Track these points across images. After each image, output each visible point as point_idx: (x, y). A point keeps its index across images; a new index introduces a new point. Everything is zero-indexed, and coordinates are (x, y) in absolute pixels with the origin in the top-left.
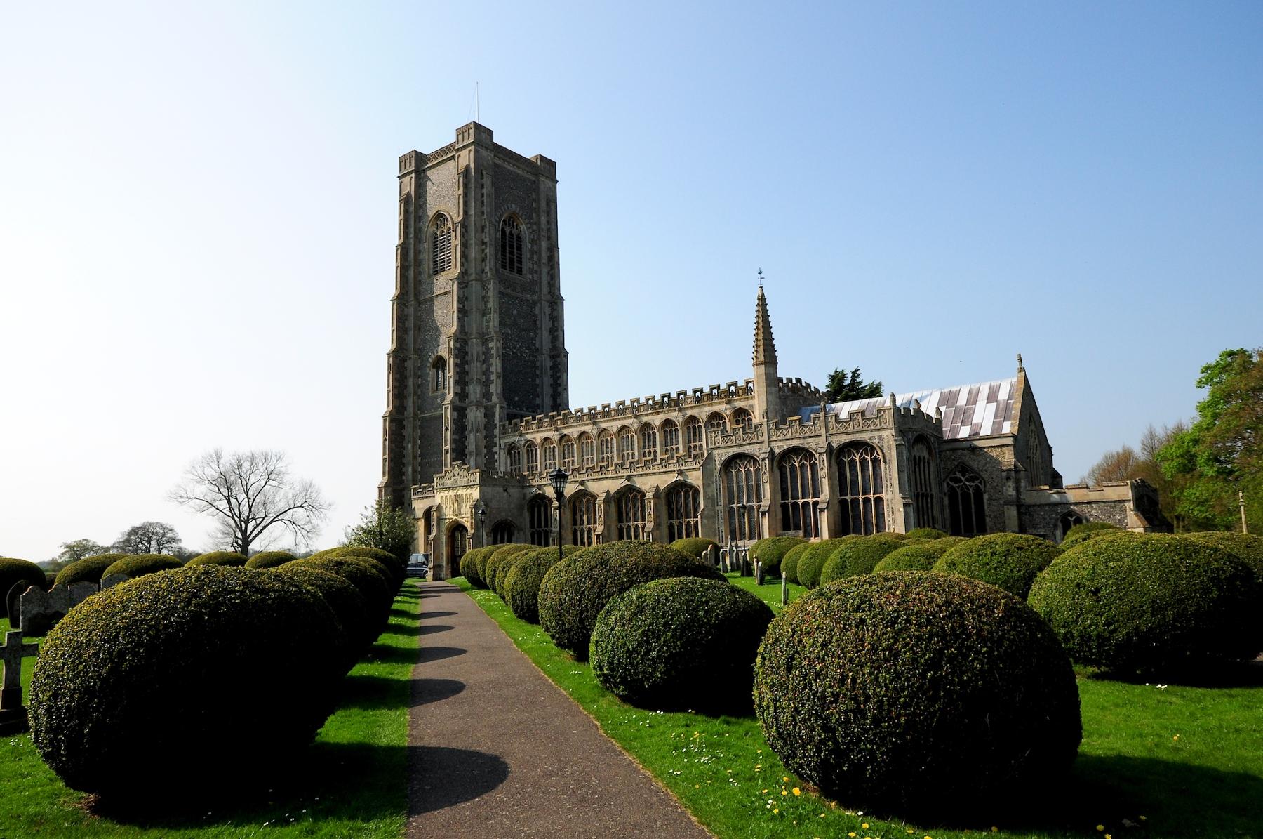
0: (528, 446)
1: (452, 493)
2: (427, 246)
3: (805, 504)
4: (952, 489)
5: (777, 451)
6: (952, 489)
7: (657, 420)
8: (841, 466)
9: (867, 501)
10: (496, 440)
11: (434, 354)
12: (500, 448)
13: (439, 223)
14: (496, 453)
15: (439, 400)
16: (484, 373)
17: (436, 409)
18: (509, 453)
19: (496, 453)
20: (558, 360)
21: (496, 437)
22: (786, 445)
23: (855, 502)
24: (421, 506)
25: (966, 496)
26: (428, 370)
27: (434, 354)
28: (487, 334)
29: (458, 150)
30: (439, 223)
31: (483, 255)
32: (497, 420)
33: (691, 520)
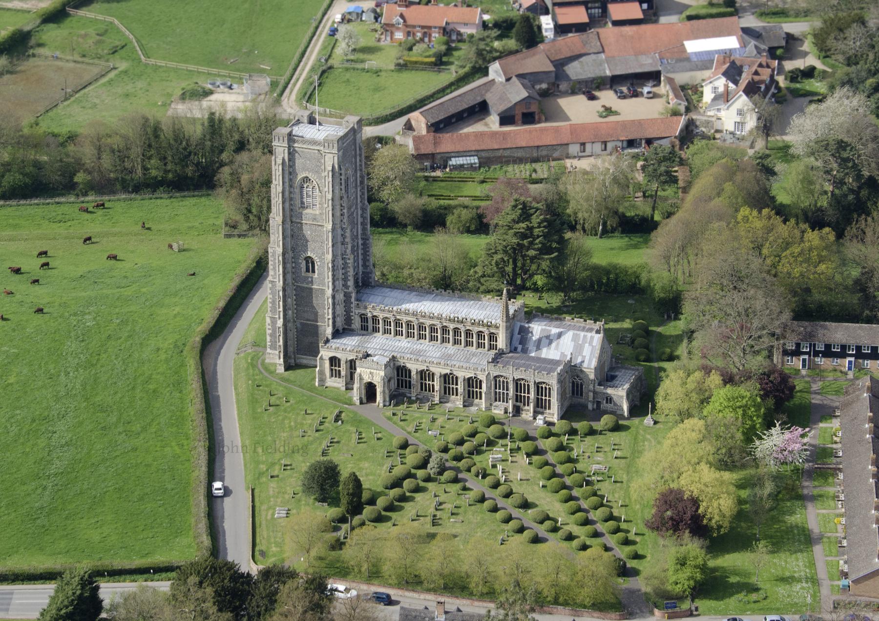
1: (369, 371)
3: (524, 396)
4: (573, 382)
5: (516, 378)
6: (573, 382)
7: (452, 326)
8: (538, 387)
9: (545, 400)
10: (353, 310)
16: (343, 274)
18: (361, 318)
20: (368, 242)
22: (519, 377)
23: (542, 399)
25: (577, 384)
32: (353, 300)
33: (478, 390)
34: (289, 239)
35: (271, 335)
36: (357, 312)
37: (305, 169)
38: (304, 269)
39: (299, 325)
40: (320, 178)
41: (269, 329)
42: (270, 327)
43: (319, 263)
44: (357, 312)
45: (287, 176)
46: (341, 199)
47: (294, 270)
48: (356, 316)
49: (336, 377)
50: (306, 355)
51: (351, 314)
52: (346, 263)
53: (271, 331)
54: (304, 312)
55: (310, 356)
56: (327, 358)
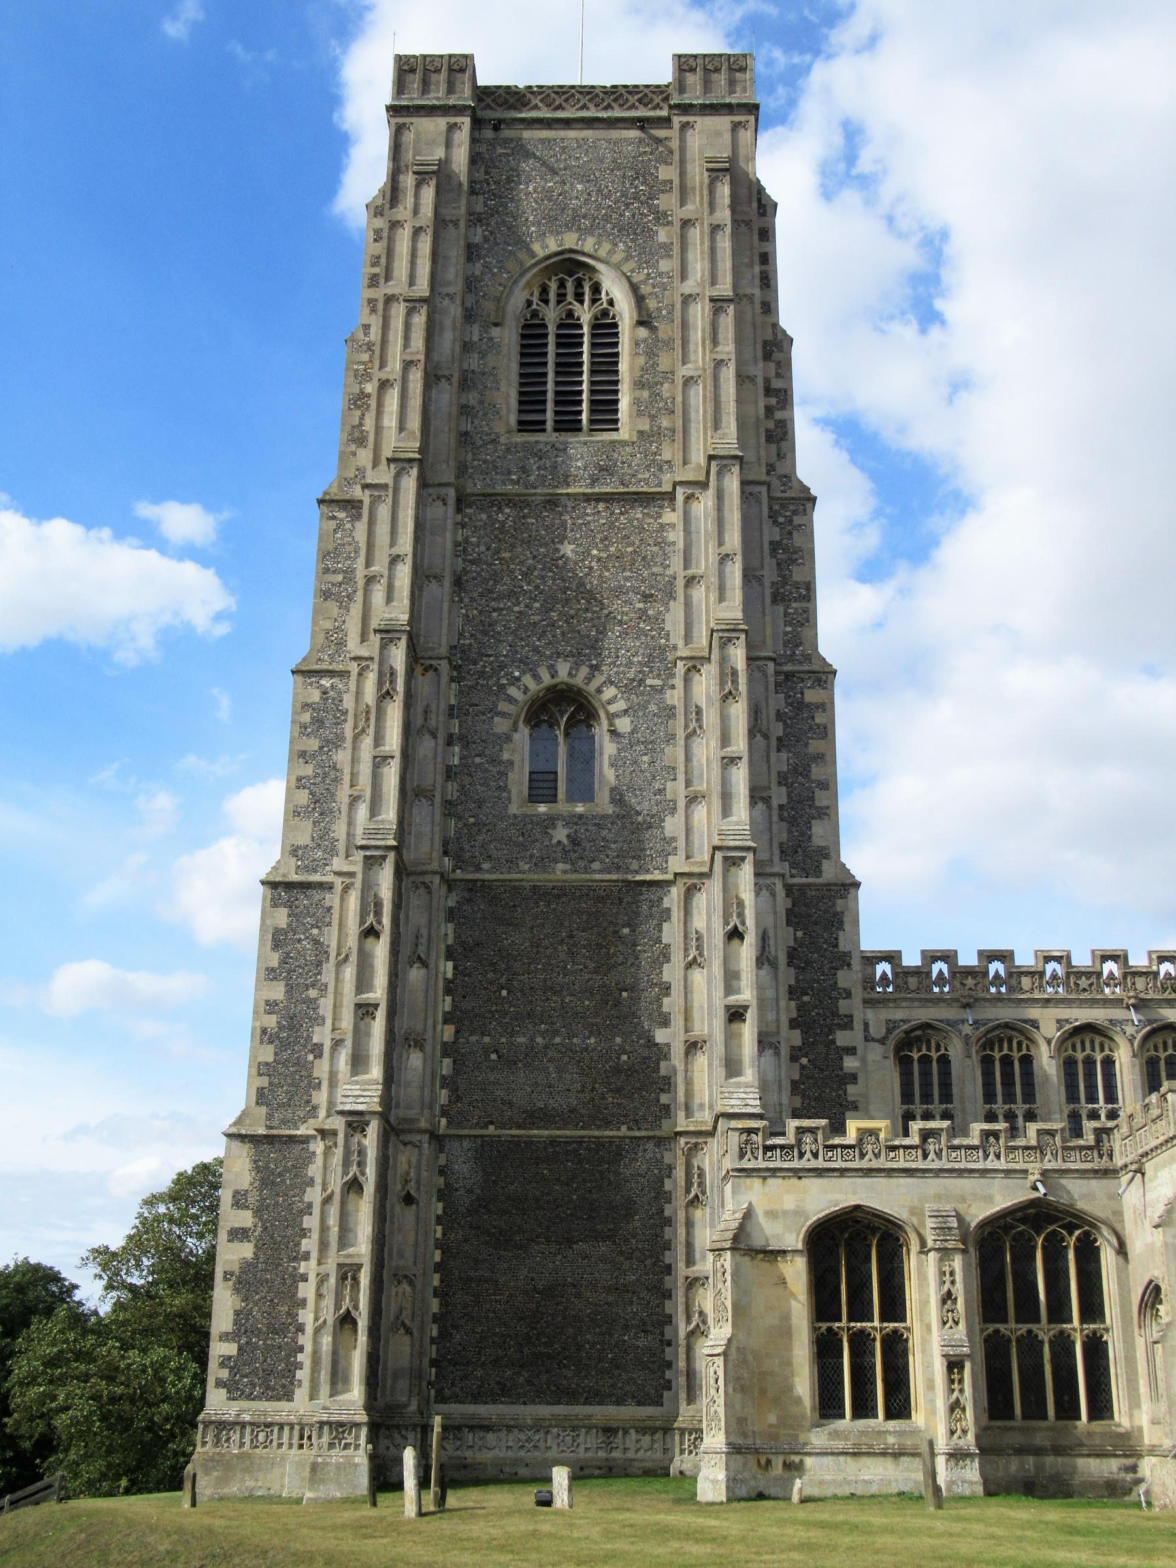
0: (988, 1044)
2: (508, 337)
11: (536, 677)
12: (867, 1039)
13: (553, 286)
14: (852, 1051)
15: (561, 834)
17: (542, 863)
18: (904, 1062)
19: (852, 1051)
21: (848, 995)
24: (789, 1203)
26: (501, 725)
27: (536, 677)
28: (791, 658)
29: (685, 109)
30: (553, 286)
31: (771, 425)
34: (441, 591)
35: (244, 1281)
36: (877, 1019)
37: (553, 222)
38: (518, 781)
39: (463, 1168)
40: (648, 253)
41: (238, 1234)
42: (245, 1219)
43: (624, 725)
44: (877, 1019)
45: (455, 253)
46: (767, 356)
47: (452, 789)
48: (875, 1053)
49: (863, 1408)
50: (503, 1393)
51: (842, 1038)
52: (799, 706)
53: (246, 1250)
54: (508, 1062)
55: (538, 1396)
56: (794, 1240)
